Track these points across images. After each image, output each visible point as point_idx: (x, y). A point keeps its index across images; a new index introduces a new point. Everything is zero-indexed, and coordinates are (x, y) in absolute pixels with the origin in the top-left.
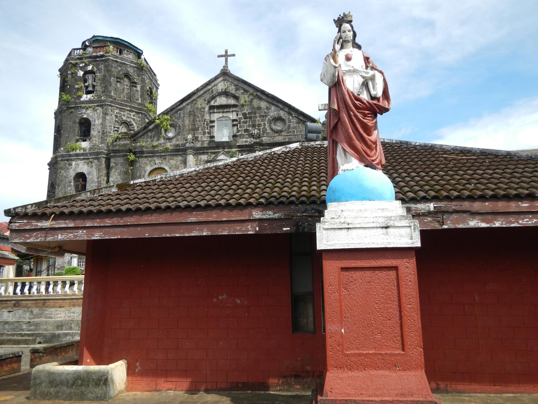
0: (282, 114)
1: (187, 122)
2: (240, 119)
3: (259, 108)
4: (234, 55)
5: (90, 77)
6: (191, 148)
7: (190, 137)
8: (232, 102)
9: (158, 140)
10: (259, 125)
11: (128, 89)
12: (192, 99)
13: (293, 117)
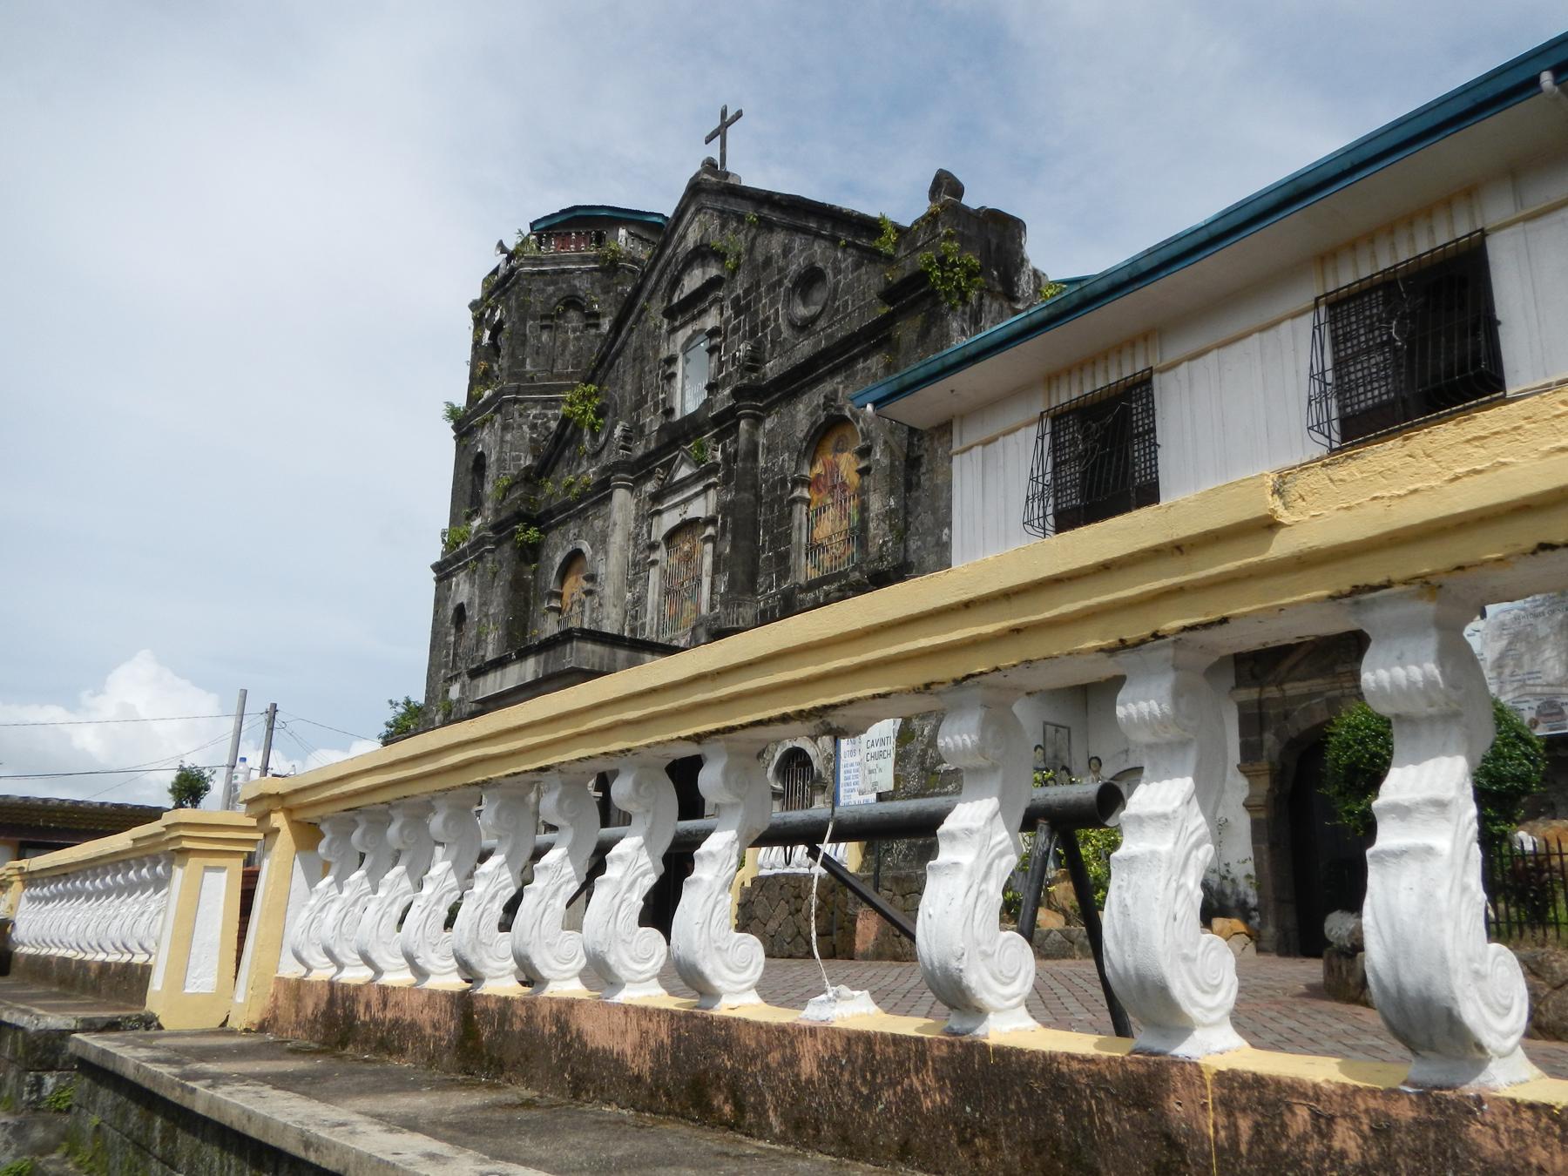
0: (818, 247)
1: (628, 387)
2: (727, 322)
3: (768, 261)
4: (739, 115)
5: (502, 338)
6: (615, 467)
7: (618, 432)
8: (713, 271)
9: (579, 465)
10: (765, 324)
11: (577, 339)
12: (636, 311)
13: (845, 248)
